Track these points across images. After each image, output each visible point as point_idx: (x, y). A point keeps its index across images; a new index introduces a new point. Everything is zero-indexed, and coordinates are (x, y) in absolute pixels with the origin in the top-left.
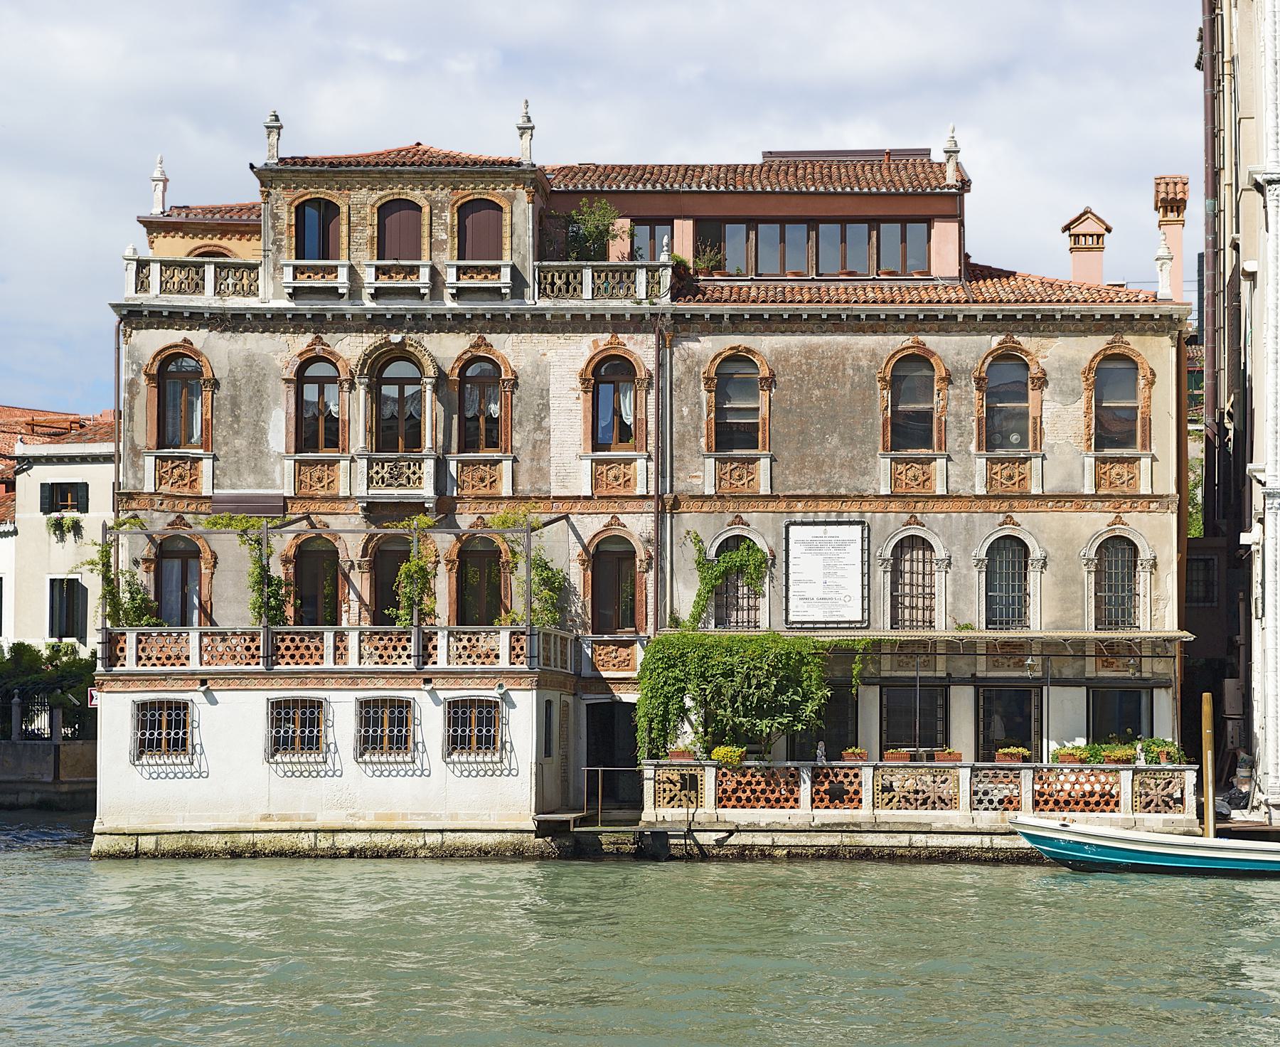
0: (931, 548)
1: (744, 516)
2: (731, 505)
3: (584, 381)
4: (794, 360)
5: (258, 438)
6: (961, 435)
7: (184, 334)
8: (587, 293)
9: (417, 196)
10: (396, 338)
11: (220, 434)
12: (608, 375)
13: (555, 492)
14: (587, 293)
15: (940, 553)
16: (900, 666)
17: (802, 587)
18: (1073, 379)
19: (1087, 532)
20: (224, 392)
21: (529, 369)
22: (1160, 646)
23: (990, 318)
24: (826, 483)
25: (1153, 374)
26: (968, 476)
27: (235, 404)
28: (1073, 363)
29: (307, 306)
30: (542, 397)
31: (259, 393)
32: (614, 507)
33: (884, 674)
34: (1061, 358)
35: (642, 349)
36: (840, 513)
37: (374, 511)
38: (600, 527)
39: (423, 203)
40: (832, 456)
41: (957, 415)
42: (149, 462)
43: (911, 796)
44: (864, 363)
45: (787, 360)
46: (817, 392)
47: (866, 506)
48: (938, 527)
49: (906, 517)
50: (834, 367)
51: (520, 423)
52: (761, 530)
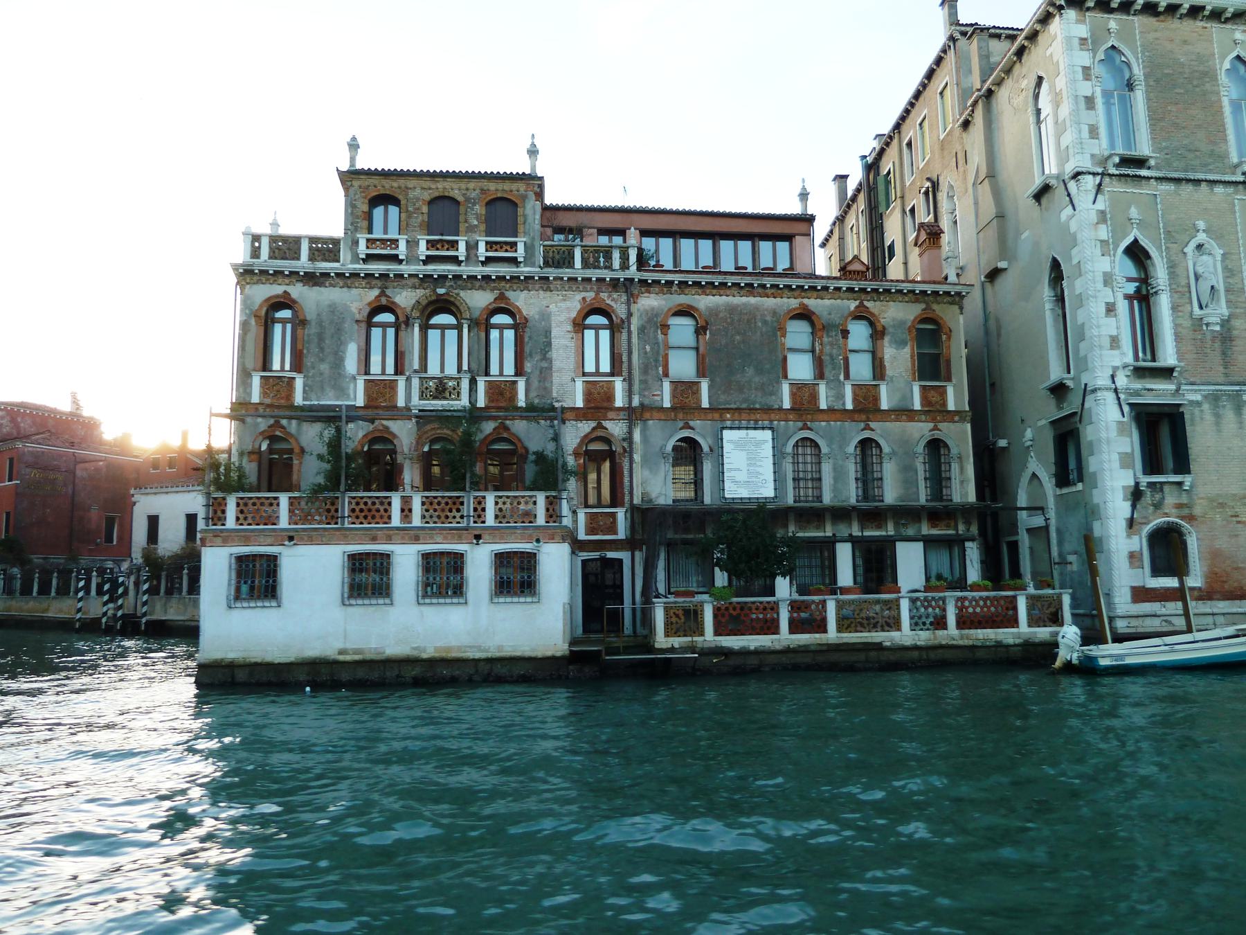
0: (817, 446)
1: (691, 423)
4: (721, 315)
5: (339, 362)
8: (578, 263)
9: (456, 194)
10: (441, 291)
11: (308, 361)
14: (578, 263)
15: (825, 449)
17: (733, 474)
19: (917, 435)
20: (312, 330)
22: (965, 511)
24: (745, 400)
26: (841, 397)
27: (321, 338)
28: (902, 323)
29: (377, 268)
31: (339, 330)
34: (894, 319)
36: (756, 421)
39: (460, 199)
41: (831, 356)
43: (865, 622)
44: (768, 318)
49: (800, 424)
51: (531, 355)
52: (700, 431)
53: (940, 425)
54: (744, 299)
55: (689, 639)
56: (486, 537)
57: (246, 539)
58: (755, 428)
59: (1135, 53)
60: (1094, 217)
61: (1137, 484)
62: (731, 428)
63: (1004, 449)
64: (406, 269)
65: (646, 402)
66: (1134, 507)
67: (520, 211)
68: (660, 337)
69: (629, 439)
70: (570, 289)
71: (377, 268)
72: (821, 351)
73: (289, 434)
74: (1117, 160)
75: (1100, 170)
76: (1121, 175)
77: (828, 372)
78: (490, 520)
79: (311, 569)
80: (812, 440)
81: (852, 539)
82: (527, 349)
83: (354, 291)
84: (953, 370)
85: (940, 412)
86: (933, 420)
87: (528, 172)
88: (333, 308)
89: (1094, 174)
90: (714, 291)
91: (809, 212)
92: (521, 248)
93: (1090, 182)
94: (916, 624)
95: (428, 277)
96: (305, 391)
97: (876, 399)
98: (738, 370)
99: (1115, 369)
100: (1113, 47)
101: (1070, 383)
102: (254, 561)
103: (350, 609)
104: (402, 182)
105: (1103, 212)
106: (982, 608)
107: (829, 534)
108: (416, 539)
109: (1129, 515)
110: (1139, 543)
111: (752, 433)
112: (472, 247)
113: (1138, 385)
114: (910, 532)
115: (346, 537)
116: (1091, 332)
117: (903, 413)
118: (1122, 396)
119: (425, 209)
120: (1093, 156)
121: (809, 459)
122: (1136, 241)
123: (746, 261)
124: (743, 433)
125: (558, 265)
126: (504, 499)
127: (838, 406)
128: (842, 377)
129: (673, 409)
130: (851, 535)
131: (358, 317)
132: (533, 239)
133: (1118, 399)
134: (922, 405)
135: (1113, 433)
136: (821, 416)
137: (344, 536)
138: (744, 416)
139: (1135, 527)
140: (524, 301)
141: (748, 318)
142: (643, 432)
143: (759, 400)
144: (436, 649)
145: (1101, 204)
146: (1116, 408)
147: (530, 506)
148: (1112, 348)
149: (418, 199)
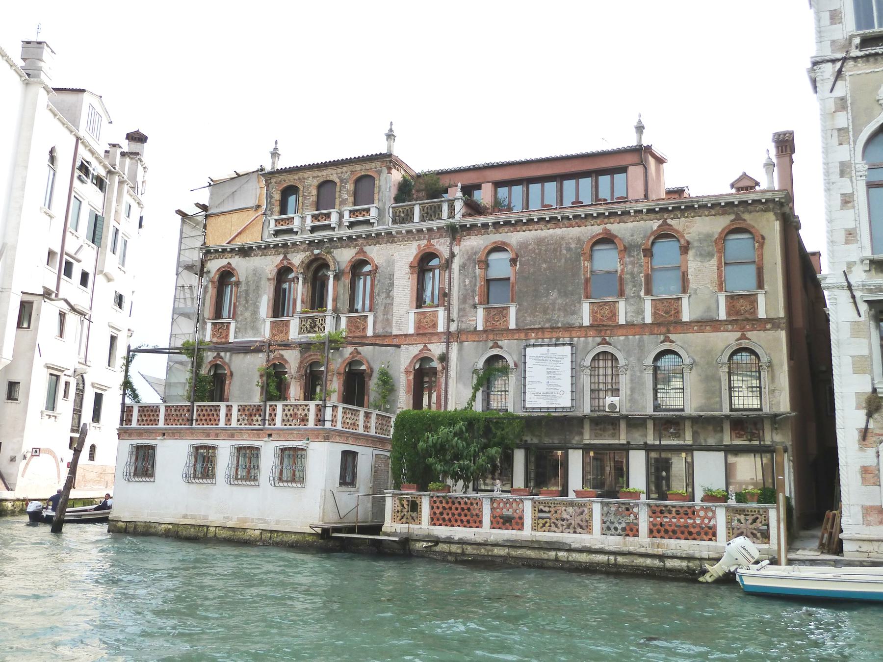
0: (614, 358)
1: (500, 343)
2: (491, 337)
3: (411, 267)
4: (531, 247)
6: (634, 286)
7: (228, 260)
8: (417, 218)
9: (335, 178)
10: (316, 252)
11: (240, 309)
12: (424, 264)
13: (395, 332)
15: (622, 362)
16: (597, 436)
17: (533, 386)
18: (708, 246)
19: (721, 345)
20: (243, 288)
21: (384, 264)
23: (651, 211)
24: (549, 320)
25: (763, 238)
26: (640, 312)
27: (247, 294)
28: (708, 236)
30: (390, 279)
31: (258, 287)
32: (425, 339)
33: (587, 442)
34: (699, 234)
35: (442, 246)
36: (558, 339)
37: (305, 347)
38: (417, 352)
39: (337, 181)
40: (553, 304)
41: (632, 274)
42: (209, 326)
44: (573, 246)
45: (526, 247)
46: (544, 265)
47: (574, 334)
48: (618, 345)
49: (599, 340)
50: (555, 250)
51: (378, 294)
52: (508, 350)
53: (749, 334)
54: (551, 231)
56: (274, 436)
58: (556, 345)
62: (534, 346)
64: (297, 238)
65: (464, 326)
67: (377, 182)
68: (478, 271)
69: (444, 358)
70: (409, 239)
72: (622, 270)
73: (225, 363)
74: (857, 41)
76: (867, 56)
77: (629, 290)
78: (279, 423)
80: (598, 354)
81: (647, 448)
82: (376, 290)
83: (269, 258)
84: (766, 277)
85: (748, 320)
86: (742, 329)
87: (384, 151)
88: (255, 272)
89: (833, 61)
90: (524, 228)
91: (645, 143)
92: (374, 212)
94: (609, 528)
95: (311, 243)
96: (236, 332)
97: (678, 312)
98: (536, 295)
99: (850, 265)
103: (192, 486)
104: (300, 175)
105: (843, 99)
106: (703, 519)
107: (623, 441)
108: (232, 436)
111: (552, 349)
112: (341, 215)
114: (711, 441)
115: (192, 434)
117: (708, 323)
118: (858, 294)
119: (314, 192)
120: (833, 42)
121: (609, 371)
123: (586, 198)
124: (544, 349)
125: (402, 221)
126: (289, 407)
127: (637, 320)
128: (642, 294)
129: (485, 331)
130: (645, 443)
131: (270, 276)
132: (385, 203)
133: (853, 297)
134: (728, 314)
136: (620, 331)
137: (192, 433)
138: (547, 335)
139: (870, 439)
140: (376, 253)
141: (556, 246)
142: (460, 350)
143: (561, 319)
144: (239, 520)
145: (841, 89)
147: (306, 412)
148: (847, 242)
149: (310, 185)
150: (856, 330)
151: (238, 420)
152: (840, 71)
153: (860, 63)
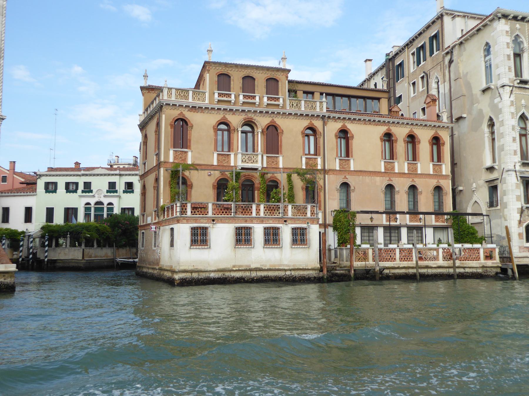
29: (223, 106)
55: (364, 263)
56: (289, 221)
57: (196, 220)
59: (525, 38)
60: (509, 103)
61: (522, 207)
63: (461, 191)
66: (521, 216)
71: (223, 106)
74: (519, 81)
75: (512, 85)
76: (519, 87)
79: (222, 233)
89: (510, 86)
93: (508, 89)
99: (515, 163)
100: (517, 35)
101: (496, 167)
102: (197, 229)
105: (512, 101)
108: (262, 222)
109: (519, 219)
110: (523, 230)
113: (523, 169)
116: (507, 148)
118: (518, 173)
120: (509, 79)
122: (523, 113)
135: (514, 187)
139: (521, 224)
145: (513, 98)
146: (515, 178)
150: (517, 186)
151: (264, 213)
152: (512, 91)
153: (517, 89)
